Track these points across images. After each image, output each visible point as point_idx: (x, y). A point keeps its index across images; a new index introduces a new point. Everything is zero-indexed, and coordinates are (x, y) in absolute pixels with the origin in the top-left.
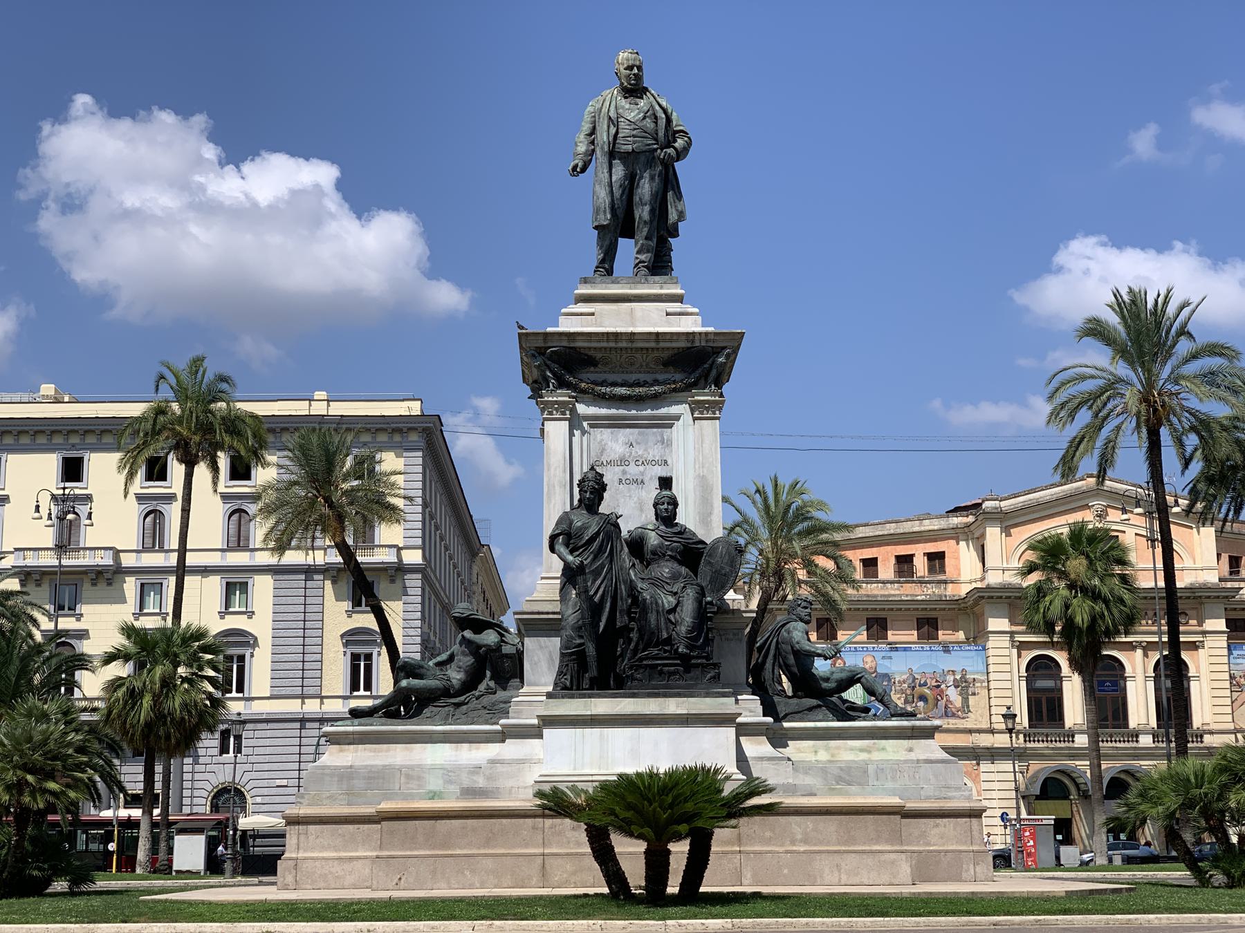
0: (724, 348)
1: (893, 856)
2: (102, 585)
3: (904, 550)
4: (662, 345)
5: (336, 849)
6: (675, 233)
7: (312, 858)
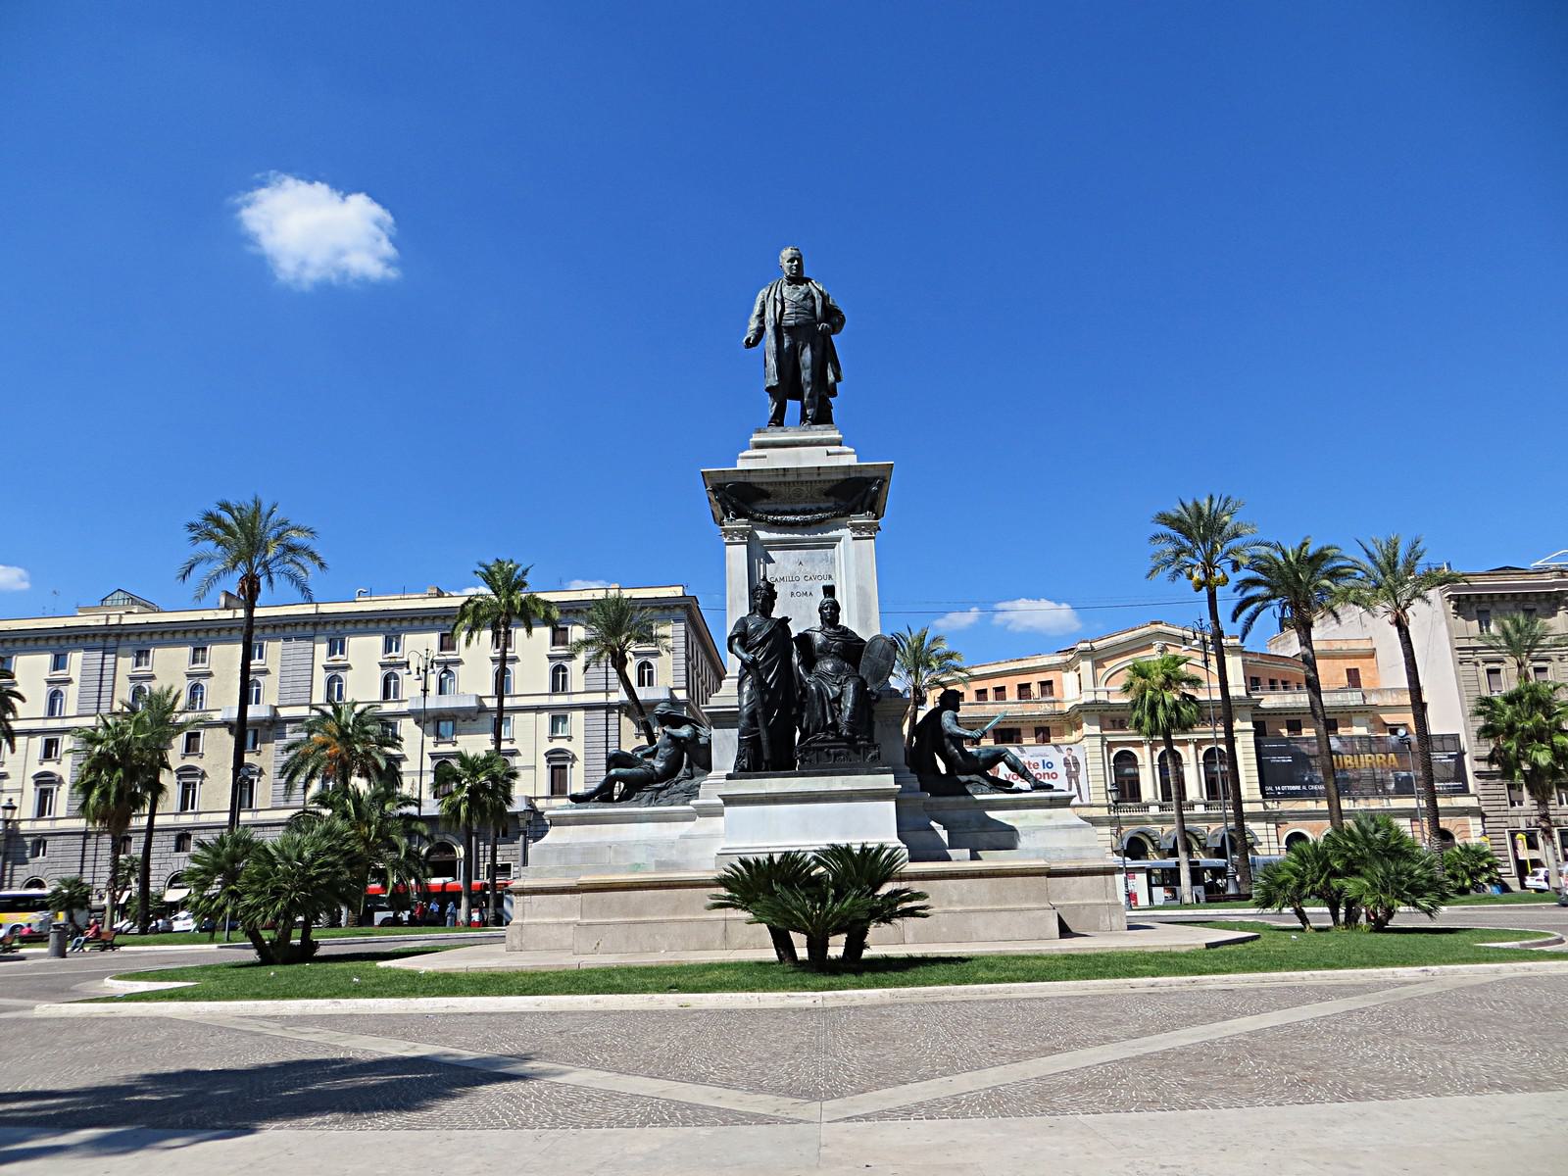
0: (876, 478)
1: (1041, 913)
3: (1023, 680)
4: (822, 478)
5: (555, 915)
6: (834, 394)
7: (536, 924)
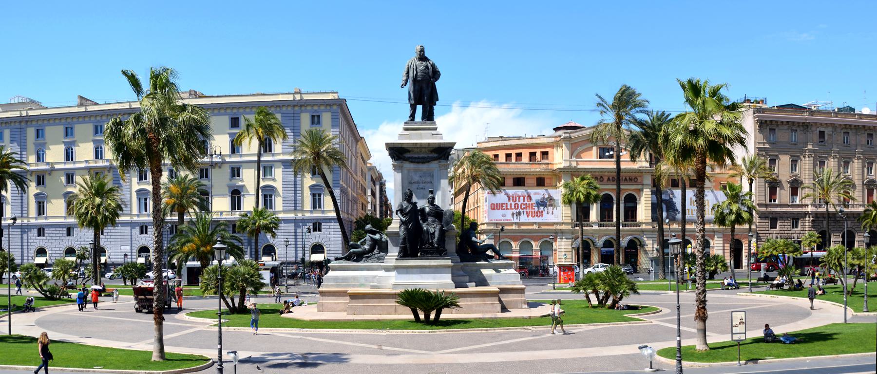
2: (217, 168)
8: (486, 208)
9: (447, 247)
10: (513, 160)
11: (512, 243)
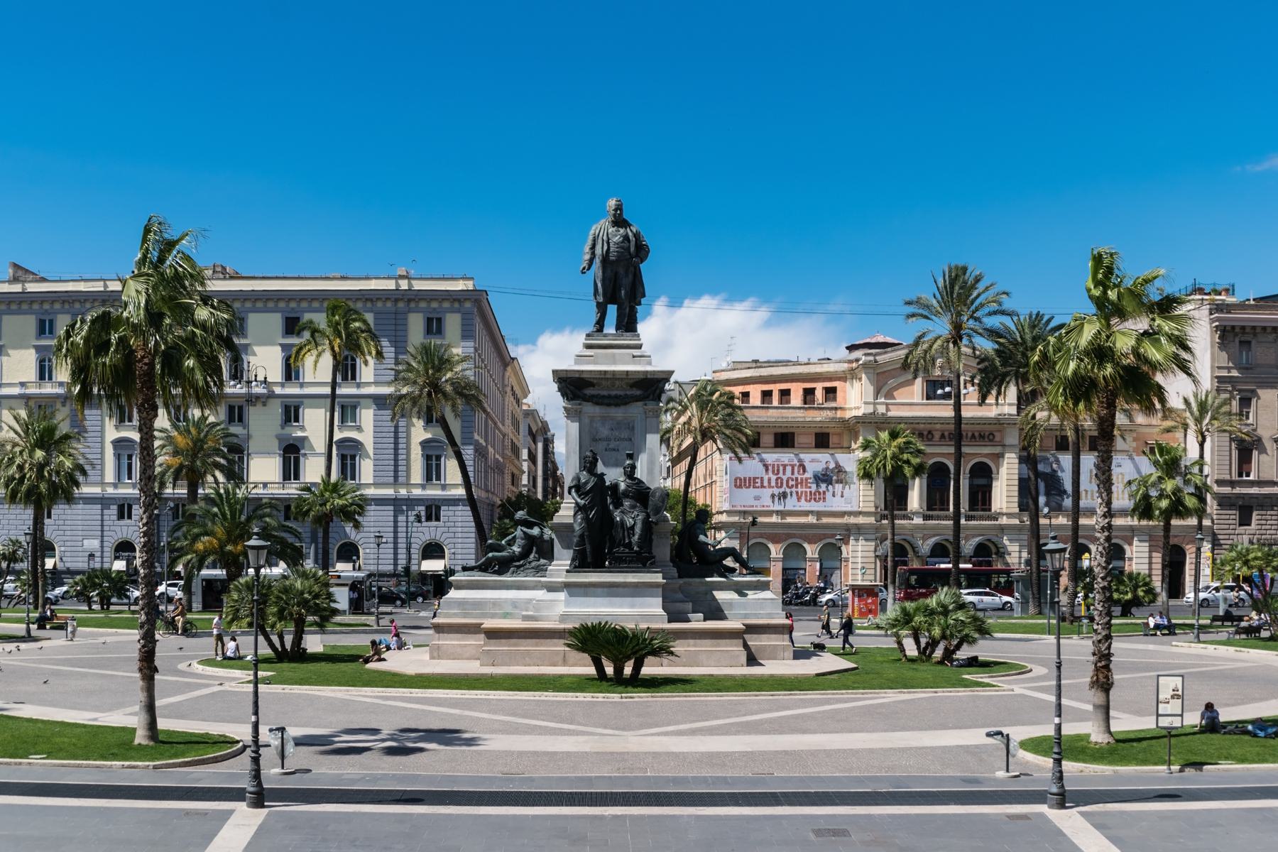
2: (259, 406)
8: (726, 485)
9: (655, 551)
10: (775, 402)
11: (771, 546)
